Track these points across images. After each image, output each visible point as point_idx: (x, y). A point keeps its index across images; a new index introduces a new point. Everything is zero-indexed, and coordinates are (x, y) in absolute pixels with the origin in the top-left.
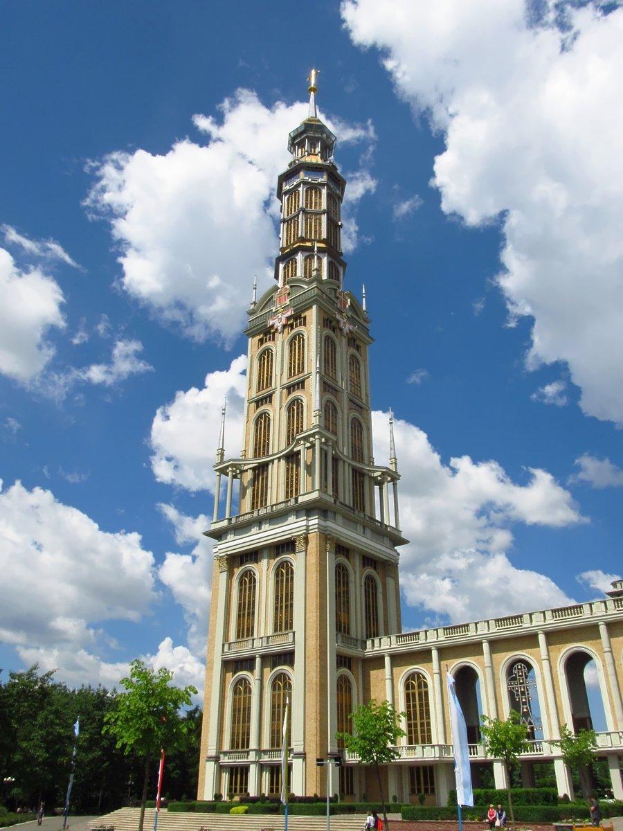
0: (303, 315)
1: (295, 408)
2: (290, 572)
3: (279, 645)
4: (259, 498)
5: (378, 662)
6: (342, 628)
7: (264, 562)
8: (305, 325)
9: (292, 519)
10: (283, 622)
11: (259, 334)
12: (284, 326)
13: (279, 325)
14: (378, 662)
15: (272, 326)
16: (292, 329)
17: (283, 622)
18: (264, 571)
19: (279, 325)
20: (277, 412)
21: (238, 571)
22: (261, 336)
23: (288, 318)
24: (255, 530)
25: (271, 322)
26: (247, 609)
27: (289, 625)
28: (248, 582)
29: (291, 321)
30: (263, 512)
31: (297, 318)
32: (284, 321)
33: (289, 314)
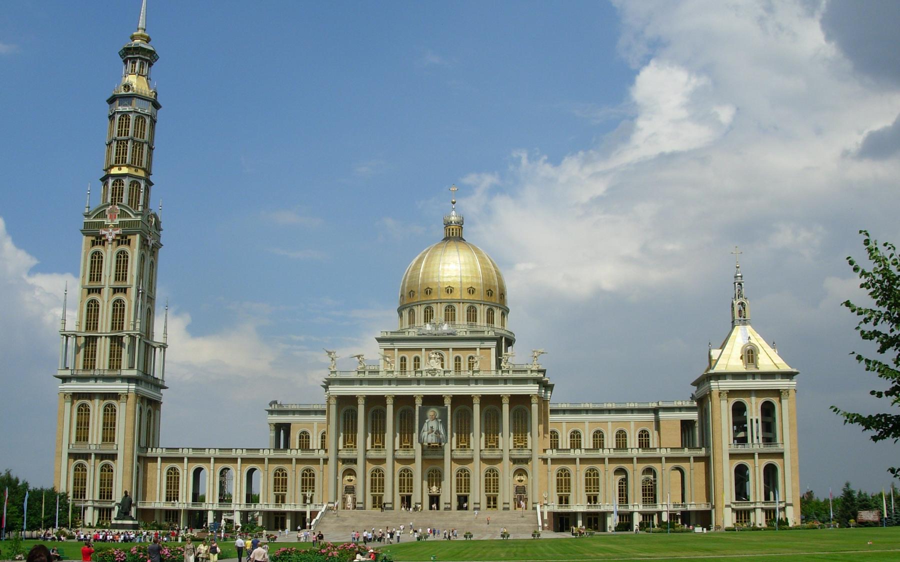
0: (129, 237)
1: (118, 308)
3: (107, 450)
7: (97, 401)
8: (129, 244)
11: (92, 236)
12: (113, 240)
13: (110, 238)
15: (104, 235)
16: (118, 245)
19: (110, 238)
20: (105, 302)
22: (94, 238)
23: (117, 235)
25: (104, 232)
27: (112, 439)
28: (84, 411)
29: (118, 238)
31: (123, 239)
33: (118, 232)
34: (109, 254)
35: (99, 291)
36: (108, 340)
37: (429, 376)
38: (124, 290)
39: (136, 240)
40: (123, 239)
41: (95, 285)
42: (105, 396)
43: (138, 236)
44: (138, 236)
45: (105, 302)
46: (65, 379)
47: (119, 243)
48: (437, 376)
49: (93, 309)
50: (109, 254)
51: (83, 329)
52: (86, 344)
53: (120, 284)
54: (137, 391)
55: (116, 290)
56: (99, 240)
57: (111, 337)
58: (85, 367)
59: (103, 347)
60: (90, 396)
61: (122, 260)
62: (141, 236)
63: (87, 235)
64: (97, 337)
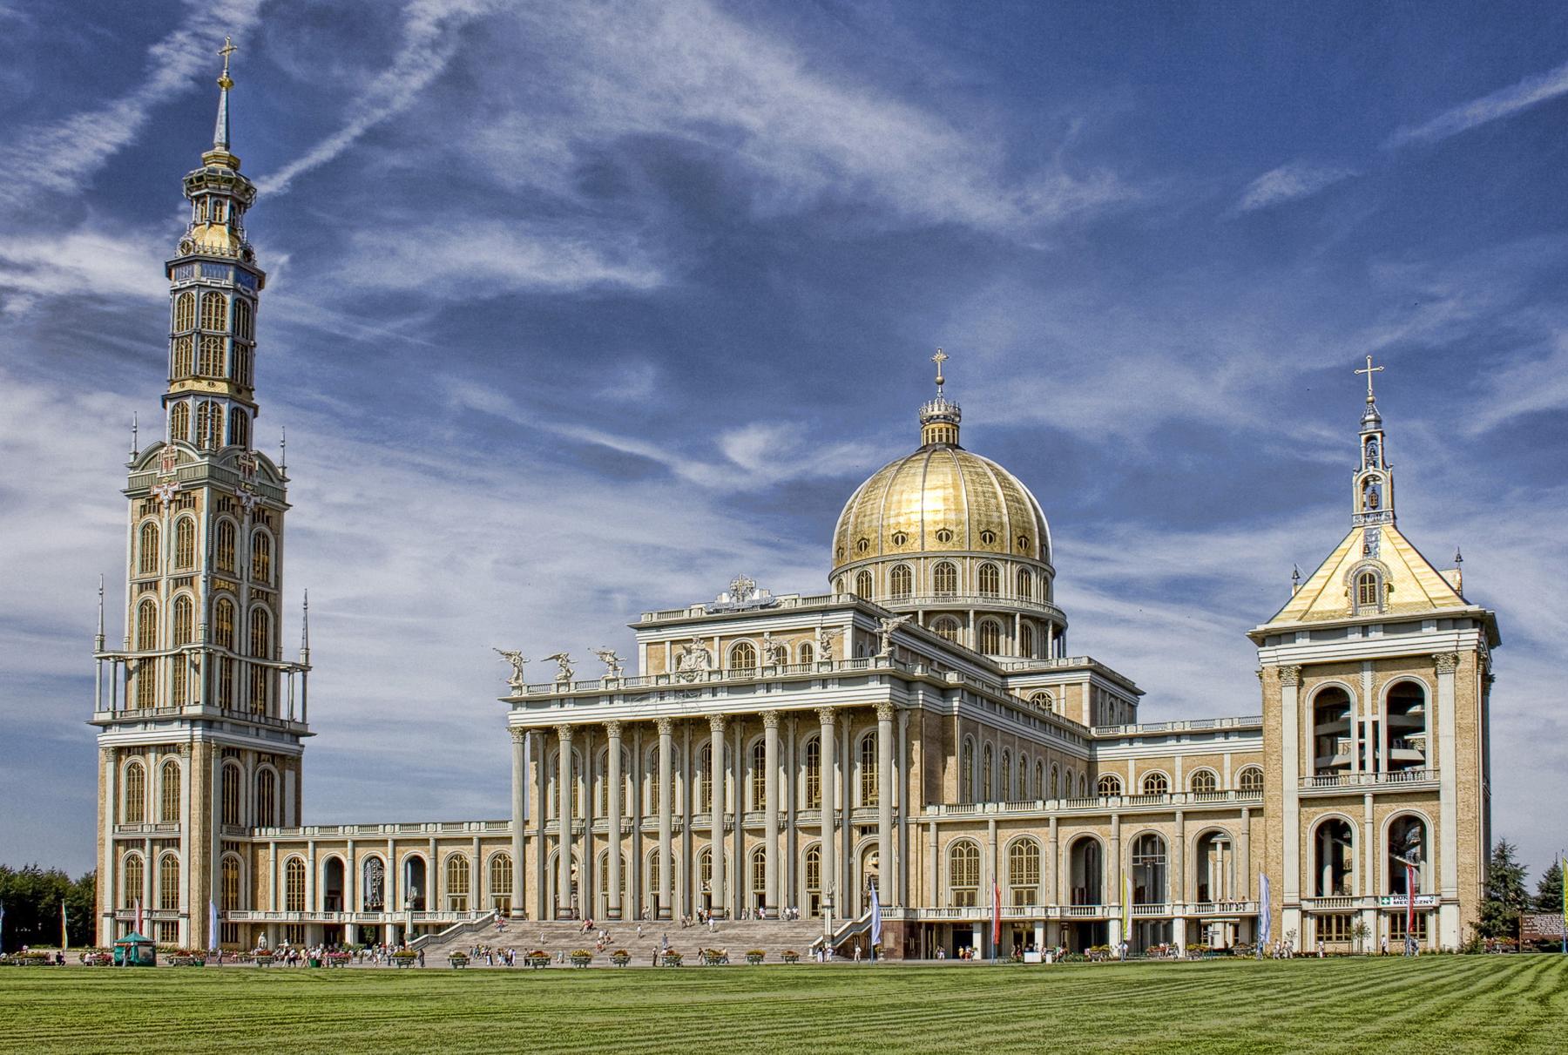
2: (177, 771)
4: (146, 695)
5: (266, 845)
6: (229, 817)
7: (152, 756)
9: (176, 725)
10: (171, 813)
13: (165, 498)
14: (266, 845)
17: (170, 815)
18: (152, 765)
19: (165, 498)
20: (163, 601)
21: (125, 762)
22: (143, 502)
23: (175, 493)
24: (140, 727)
25: (156, 491)
26: (136, 798)
27: (177, 817)
28: (136, 774)
29: (178, 497)
30: (148, 714)
31: (184, 498)
32: (170, 495)
33: (176, 488)
34: (165, 523)
35: (153, 585)
36: (170, 660)
37: (683, 682)
38: (189, 581)
39: (203, 495)
40: (184, 498)
41: (148, 576)
42: (165, 748)
43: (205, 489)
44: (205, 489)
45: (163, 601)
46: (106, 726)
47: (181, 505)
48: (697, 681)
49: (147, 611)
50: (165, 523)
51: (135, 646)
52: (140, 668)
53: (182, 572)
54: (206, 741)
55: (179, 582)
56: (151, 504)
57: (174, 656)
58: (140, 706)
59: (164, 671)
60: (143, 750)
61: (184, 528)
62: (213, 490)
63: (134, 497)
64: (152, 659)
